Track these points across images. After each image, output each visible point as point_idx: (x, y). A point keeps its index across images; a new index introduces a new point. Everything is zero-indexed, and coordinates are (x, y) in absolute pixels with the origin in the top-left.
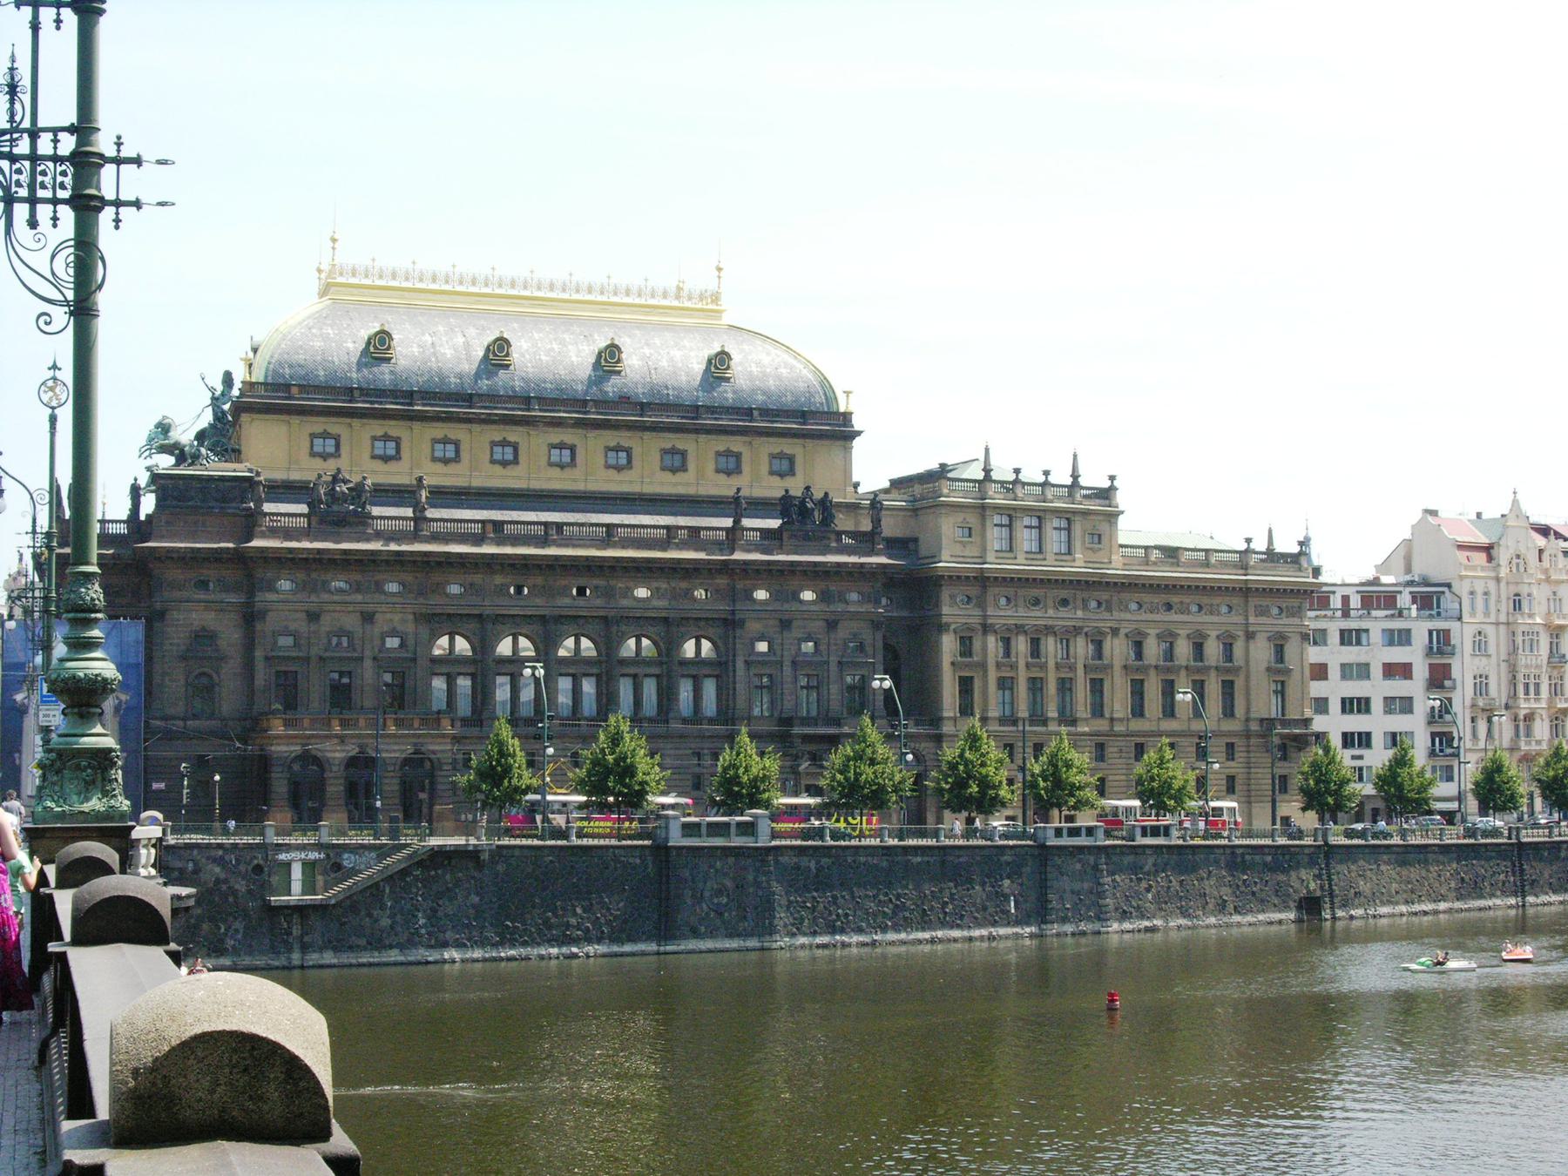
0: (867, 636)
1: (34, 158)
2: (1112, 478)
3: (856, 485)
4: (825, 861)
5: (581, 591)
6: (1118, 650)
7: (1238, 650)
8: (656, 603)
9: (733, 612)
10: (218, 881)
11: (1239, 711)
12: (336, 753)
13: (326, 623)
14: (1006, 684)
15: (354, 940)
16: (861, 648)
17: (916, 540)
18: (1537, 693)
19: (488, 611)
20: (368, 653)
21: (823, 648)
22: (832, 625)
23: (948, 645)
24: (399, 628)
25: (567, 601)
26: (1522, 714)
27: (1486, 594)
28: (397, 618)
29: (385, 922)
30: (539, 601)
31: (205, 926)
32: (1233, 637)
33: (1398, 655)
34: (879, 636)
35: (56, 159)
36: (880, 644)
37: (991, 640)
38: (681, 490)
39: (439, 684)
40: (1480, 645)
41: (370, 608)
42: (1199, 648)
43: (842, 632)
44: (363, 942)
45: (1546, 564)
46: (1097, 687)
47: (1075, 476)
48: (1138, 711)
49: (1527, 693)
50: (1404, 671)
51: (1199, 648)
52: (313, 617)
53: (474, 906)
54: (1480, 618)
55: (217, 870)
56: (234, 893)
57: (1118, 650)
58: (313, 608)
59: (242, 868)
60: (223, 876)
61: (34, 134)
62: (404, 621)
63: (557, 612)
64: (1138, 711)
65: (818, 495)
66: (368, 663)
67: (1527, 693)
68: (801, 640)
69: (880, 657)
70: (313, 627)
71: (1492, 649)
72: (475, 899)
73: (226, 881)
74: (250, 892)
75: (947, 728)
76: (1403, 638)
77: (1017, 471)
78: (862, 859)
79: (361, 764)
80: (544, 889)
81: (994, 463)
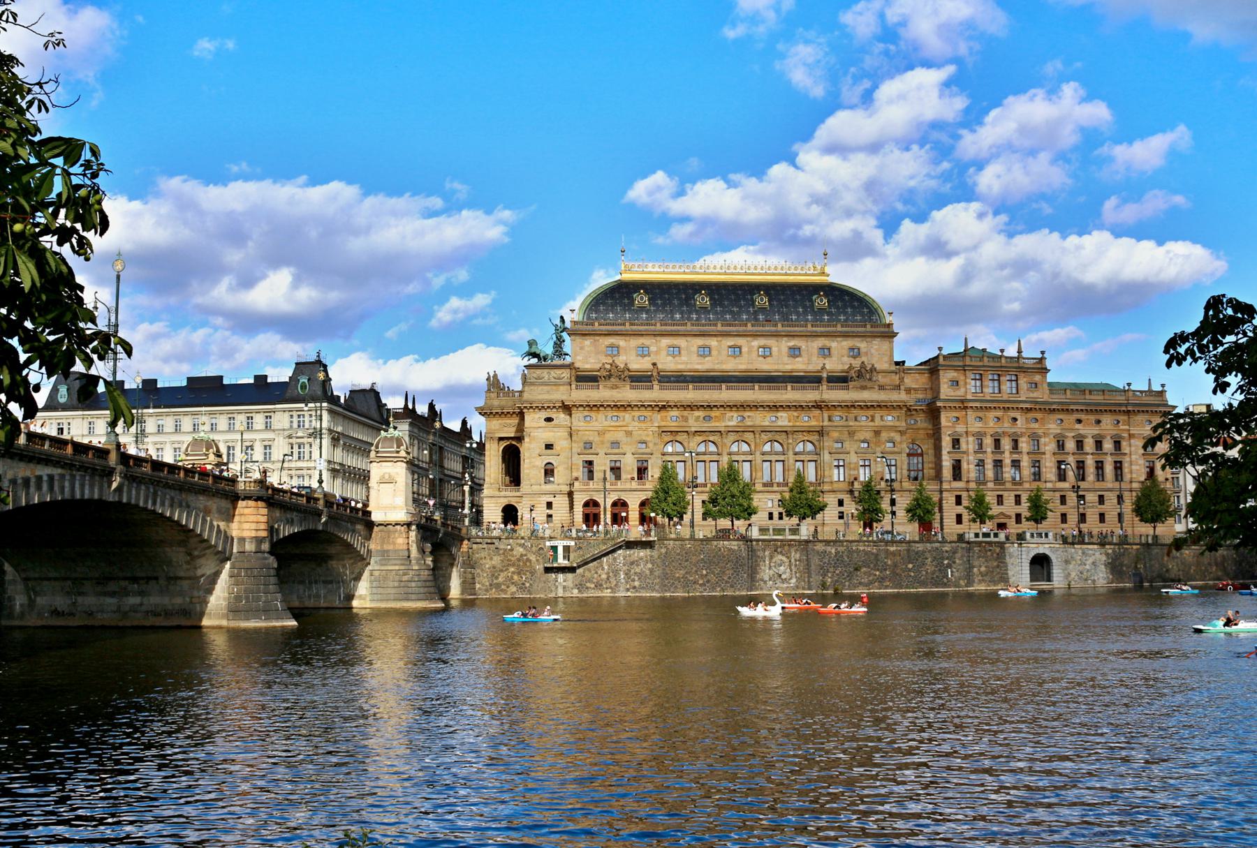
2: (1043, 353)
6: (1049, 446)
7: (1124, 444)
10: (522, 555)
11: (1127, 477)
14: (981, 463)
29: (604, 576)
31: (516, 577)
32: (1123, 438)
37: (971, 439)
42: (1099, 444)
47: (1019, 352)
51: (1099, 444)
56: (528, 560)
59: (534, 549)
72: (650, 566)
75: (945, 486)
79: (620, 504)
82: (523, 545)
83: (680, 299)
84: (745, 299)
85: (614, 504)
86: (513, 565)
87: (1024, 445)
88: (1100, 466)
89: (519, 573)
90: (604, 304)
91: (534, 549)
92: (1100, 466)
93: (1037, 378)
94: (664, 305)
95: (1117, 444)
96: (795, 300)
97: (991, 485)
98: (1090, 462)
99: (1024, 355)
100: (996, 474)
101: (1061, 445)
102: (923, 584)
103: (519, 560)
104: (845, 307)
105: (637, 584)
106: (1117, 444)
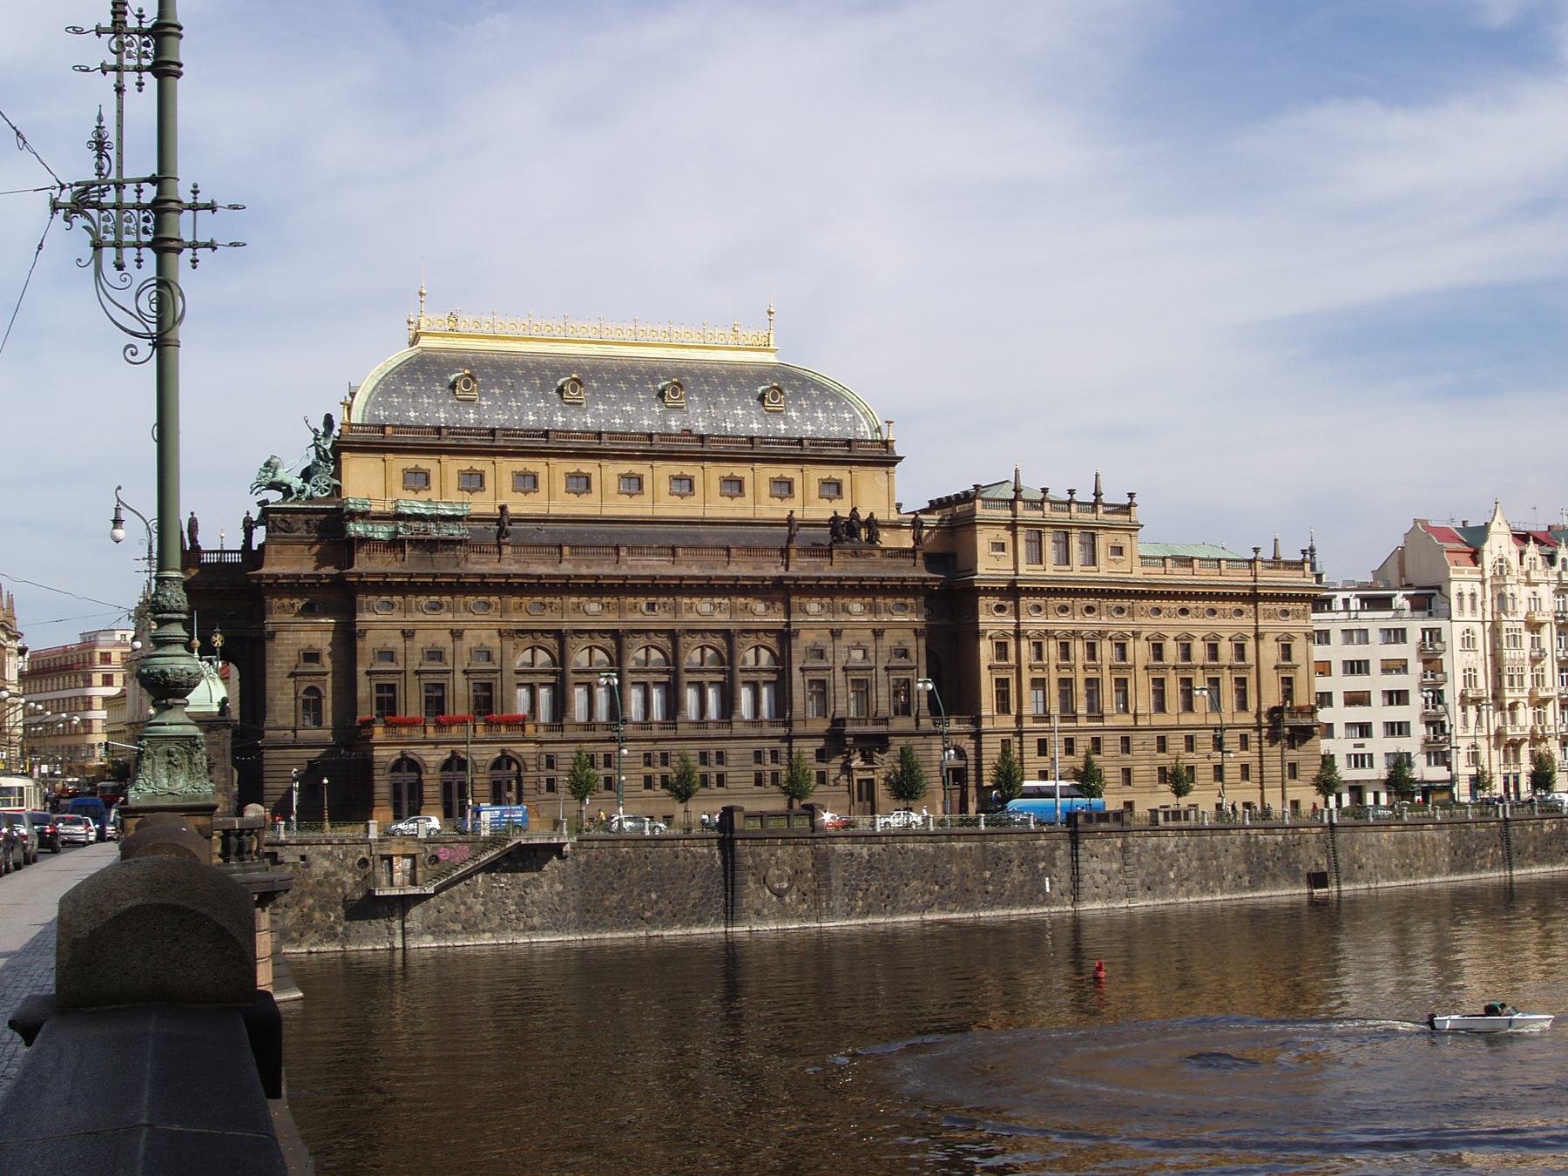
0: (911, 643)
1: (118, 206)
3: (899, 506)
4: (877, 848)
5: (651, 606)
6: (1139, 652)
8: (718, 616)
9: (788, 624)
10: (327, 874)
12: (433, 757)
13: (421, 641)
15: (451, 926)
16: (905, 653)
17: (954, 555)
18: (1521, 683)
19: (566, 627)
20: (459, 668)
21: (871, 654)
22: (878, 634)
23: (986, 649)
24: (486, 643)
25: (638, 616)
26: (1508, 702)
27: (1473, 595)
28: (484, 634)
29: (479, 908)
30: (612, 617)
31: (317, 915)
33: (1395, 651)
34: (922, 642)
35: (139, 207)
36: (923, 650)
38: (740, 514)
39: (523, 694)
40: (1468, 642)
41: (460, 626)
42: (1213, 651)
43: (889, 640)
44: (458, 927)
45: (1526, 567)
46: (1122, 684)
47: (1097, 494)
48: (1160, 707)
49: (1512, 684)
50: (1401, 667)
51: (1213, 651)
52: (407, 635)
53: (558, 894)
54: (1468, 615)
55: (327, 864)
56: (343, 885)
57: (1139, 652)
58: (409, 627)
59: (349, 861)
60: (332, 869)
61: (120, 186)
62: (491, 637)
63: (629, 627)
64: (1160, 707)
65: (864, 516)
66: (459, 676)
67: (1512, 684)
68: (850, 648)
69: (923, 662)
70: (409, 644)
71: (1479, 645)
72: (559, 887)
73: (334, 874)
74: (357, 884)
76: (1399, 635)
77: (1045, 491)
78: (910, 846)
80: (622, 877)
81: (1023, 483)
82: (328, 856)
83: (532, 387)
84: (645, 391)
85: (447, 766)
86: (312, 894)
87: (1106, 651)
88: (1187, 686)
89: (323, 909)
90: (399, 392)
91: (349, 861)
92: (1187, 686)
93: (1123, 539)
94: (506, 397)
95: (1240, 649)
96: (729, 395)
97: (1056, 723)
98: (1200, 681)
99: (1105, 499)
100: (1091, 708)
101: (1158, 651)
102: (1010, 903)
103: (320, 883)
104: (814, 408)
105: (536, 920)
106: (1240, 649)
